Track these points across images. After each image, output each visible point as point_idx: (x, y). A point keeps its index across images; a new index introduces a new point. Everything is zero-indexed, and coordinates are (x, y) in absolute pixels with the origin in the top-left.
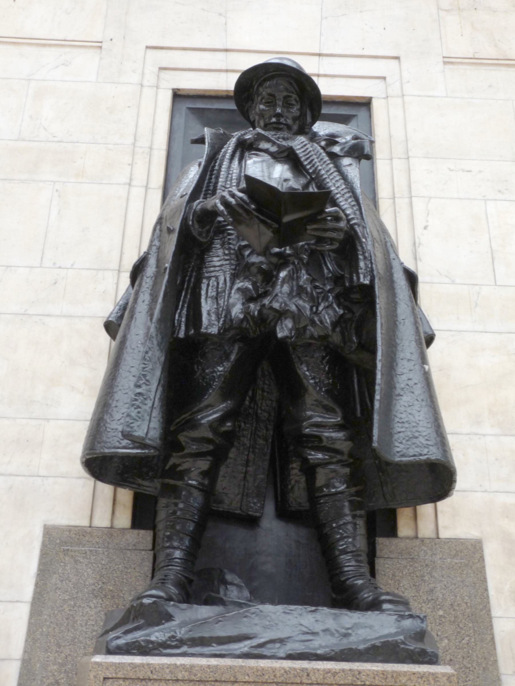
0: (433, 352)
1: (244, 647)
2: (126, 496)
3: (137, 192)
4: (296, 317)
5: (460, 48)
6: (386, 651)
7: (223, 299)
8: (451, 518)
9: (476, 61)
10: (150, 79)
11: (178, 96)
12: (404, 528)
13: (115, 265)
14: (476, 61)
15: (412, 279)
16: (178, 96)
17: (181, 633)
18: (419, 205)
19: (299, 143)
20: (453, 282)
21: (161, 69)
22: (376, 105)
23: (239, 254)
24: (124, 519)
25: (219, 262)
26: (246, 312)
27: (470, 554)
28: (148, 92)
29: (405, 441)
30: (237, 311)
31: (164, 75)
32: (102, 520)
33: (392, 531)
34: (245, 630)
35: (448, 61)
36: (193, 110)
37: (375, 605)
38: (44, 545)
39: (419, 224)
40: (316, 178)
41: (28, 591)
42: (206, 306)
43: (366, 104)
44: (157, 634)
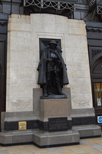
0: (67, 71)
1: (55, 98)
2: (40, 85)
3: (37, 52)
4: (56, 71)
5: (70, 32)
6: (64, 98)
7: (50, 69)
8: (68, 86)
9: (72, 34)
10: (36, 37)
11: (40, 39)
12: (64, 87)
13: (36, 61)
14: (72, 34)
15: (66, 65)
16: (40, 39)
17: (50, 97)
18: (66, 54)
19: (56, 52)
20: (69, 62)
21: (38, 35)
22: (61, 40)
23: (51, 64)
24: (40, 87)
25: (49, 65)
26: (52, 70)
27: (69, 89)
28: (36, 39)
29: (65, 82)
30: (51, 70)
31: (38, 36)
32: (38, 87)
33: (63, 87)
34: (54, 97)
35: (69, 34)
36: (41, 41)
37: (63, 94)
38: (33, 90)
39: (66, 56)
40: (58, 57)
41: (32, 94)
42: (48, 70)
43: (60, 40)
44: (48, 98)
